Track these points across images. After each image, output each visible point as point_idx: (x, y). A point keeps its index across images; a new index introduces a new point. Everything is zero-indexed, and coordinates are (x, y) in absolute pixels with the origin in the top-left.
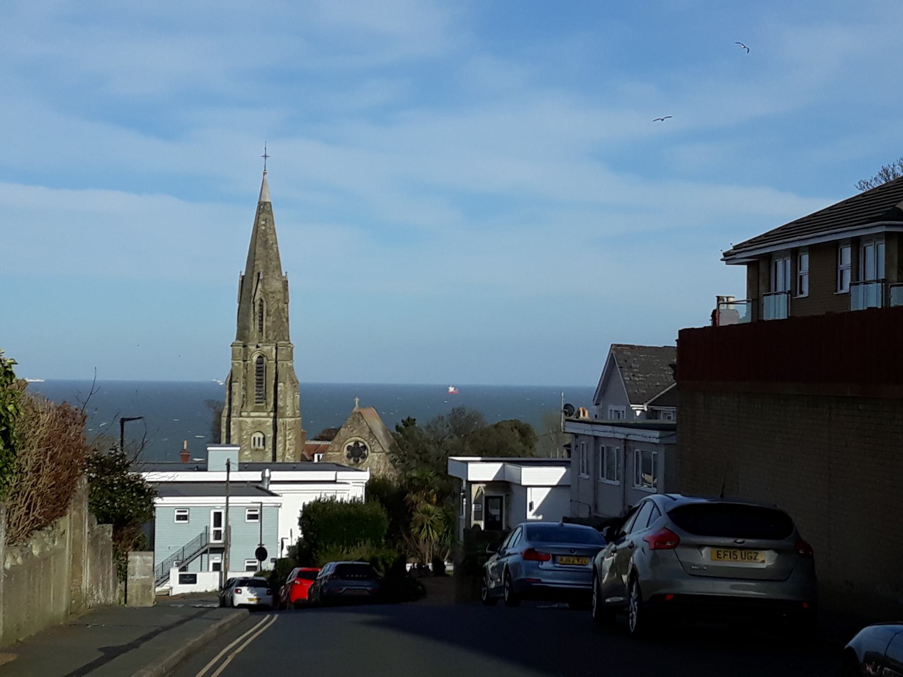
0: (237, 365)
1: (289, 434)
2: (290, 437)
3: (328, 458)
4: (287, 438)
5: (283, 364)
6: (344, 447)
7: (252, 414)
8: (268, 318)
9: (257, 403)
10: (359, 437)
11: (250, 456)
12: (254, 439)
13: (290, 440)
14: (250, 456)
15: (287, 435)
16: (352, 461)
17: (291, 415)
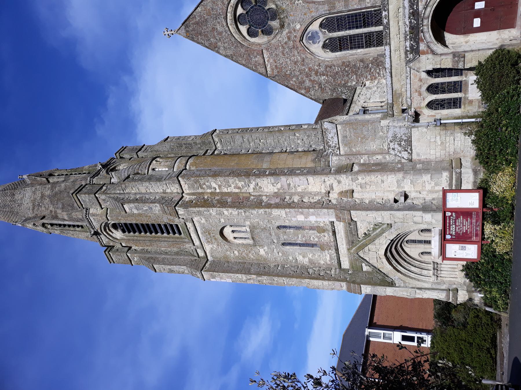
0: (136, 259)
1: (210, 187)
2: (214, 185)
3: (278, 72)
4: (218, 191)
5: (104, 200)
6: (253, 44)
7: (197, 243)
8: (60, 216)
9: (180, 233)
10: (226, 18)
11: (266, 248)
12: (235, 238)
13: (220, 186)
14: (266, 248)
15: (213, 190)
16: (275, 24)
17: (177, 186)
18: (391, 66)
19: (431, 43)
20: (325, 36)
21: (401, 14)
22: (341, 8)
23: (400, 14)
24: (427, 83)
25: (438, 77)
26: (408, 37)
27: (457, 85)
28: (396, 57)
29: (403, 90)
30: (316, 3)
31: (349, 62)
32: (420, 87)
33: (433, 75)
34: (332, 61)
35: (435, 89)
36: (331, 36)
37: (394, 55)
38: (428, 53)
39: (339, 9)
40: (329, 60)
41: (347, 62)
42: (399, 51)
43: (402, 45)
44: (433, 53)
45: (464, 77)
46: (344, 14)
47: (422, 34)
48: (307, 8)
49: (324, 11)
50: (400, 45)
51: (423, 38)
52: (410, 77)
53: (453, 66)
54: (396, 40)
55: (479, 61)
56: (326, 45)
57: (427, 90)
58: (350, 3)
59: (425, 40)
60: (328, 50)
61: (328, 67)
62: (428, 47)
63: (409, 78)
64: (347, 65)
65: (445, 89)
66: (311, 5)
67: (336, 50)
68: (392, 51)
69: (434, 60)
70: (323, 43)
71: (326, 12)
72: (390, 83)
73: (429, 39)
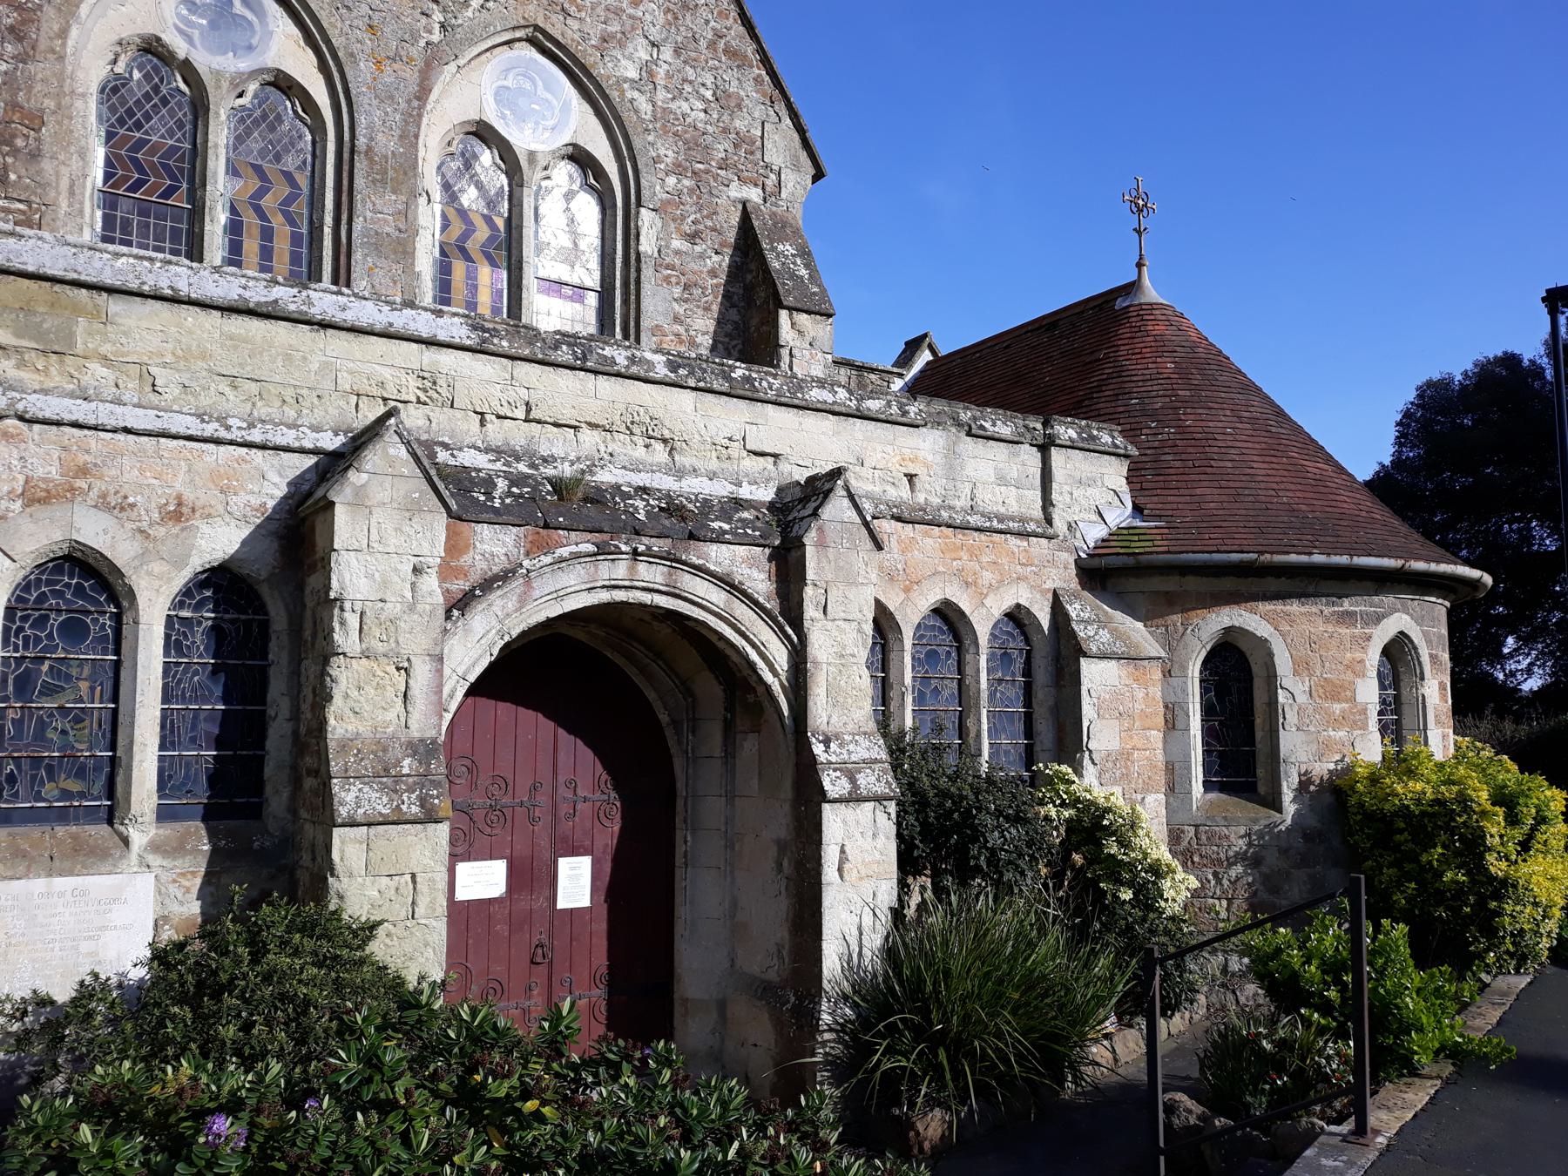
18: (325, 325)
19: (522, 601)
20: (225, 85)
21: (640, 452)
22: (369, 214)
23: (640, 441)
24: (143, 556)
25: (172, 644)
26: (522, 467)
27: (74, 786)
28: (387, 373)
29: (98, 370)
30: (415, 103)
31: (35, 155)
32: (120, 507)
33: (198, 607)
34: (61, 58)
35: (55, 620)
36: (217, 114)
37: (399, 362)
38: (447, 571)
39: (363, 200)
40: (70, 43)
41: (37, 139)
42: (423, 398)
43: (462, 426)
44: (460, 604)
45: (153, 831)
46: (328, 219)
47: (591, 548)
48: (403, 53)
49: (370, 127)
50: (459, 414)
51: (564, 552)
52: (218, 442)
53: (344, 746)
54: (495, 398)
55: (380, 923)
56: (156, 69)
57: (67, 558)
58: (383, 263)
59: (547, 559)
60: (120, 68)
61: (24, 22)
62: (488, 584)
63: (210, 429)
64: (14, 136)
65: (49, 691)
66: (411, 76)
67: (112, 109)
68: (431, 356)
69: (412, 608)
70: (181, 55)
71: (361, 131)
72: (184, 290)
73: (545, 585)
